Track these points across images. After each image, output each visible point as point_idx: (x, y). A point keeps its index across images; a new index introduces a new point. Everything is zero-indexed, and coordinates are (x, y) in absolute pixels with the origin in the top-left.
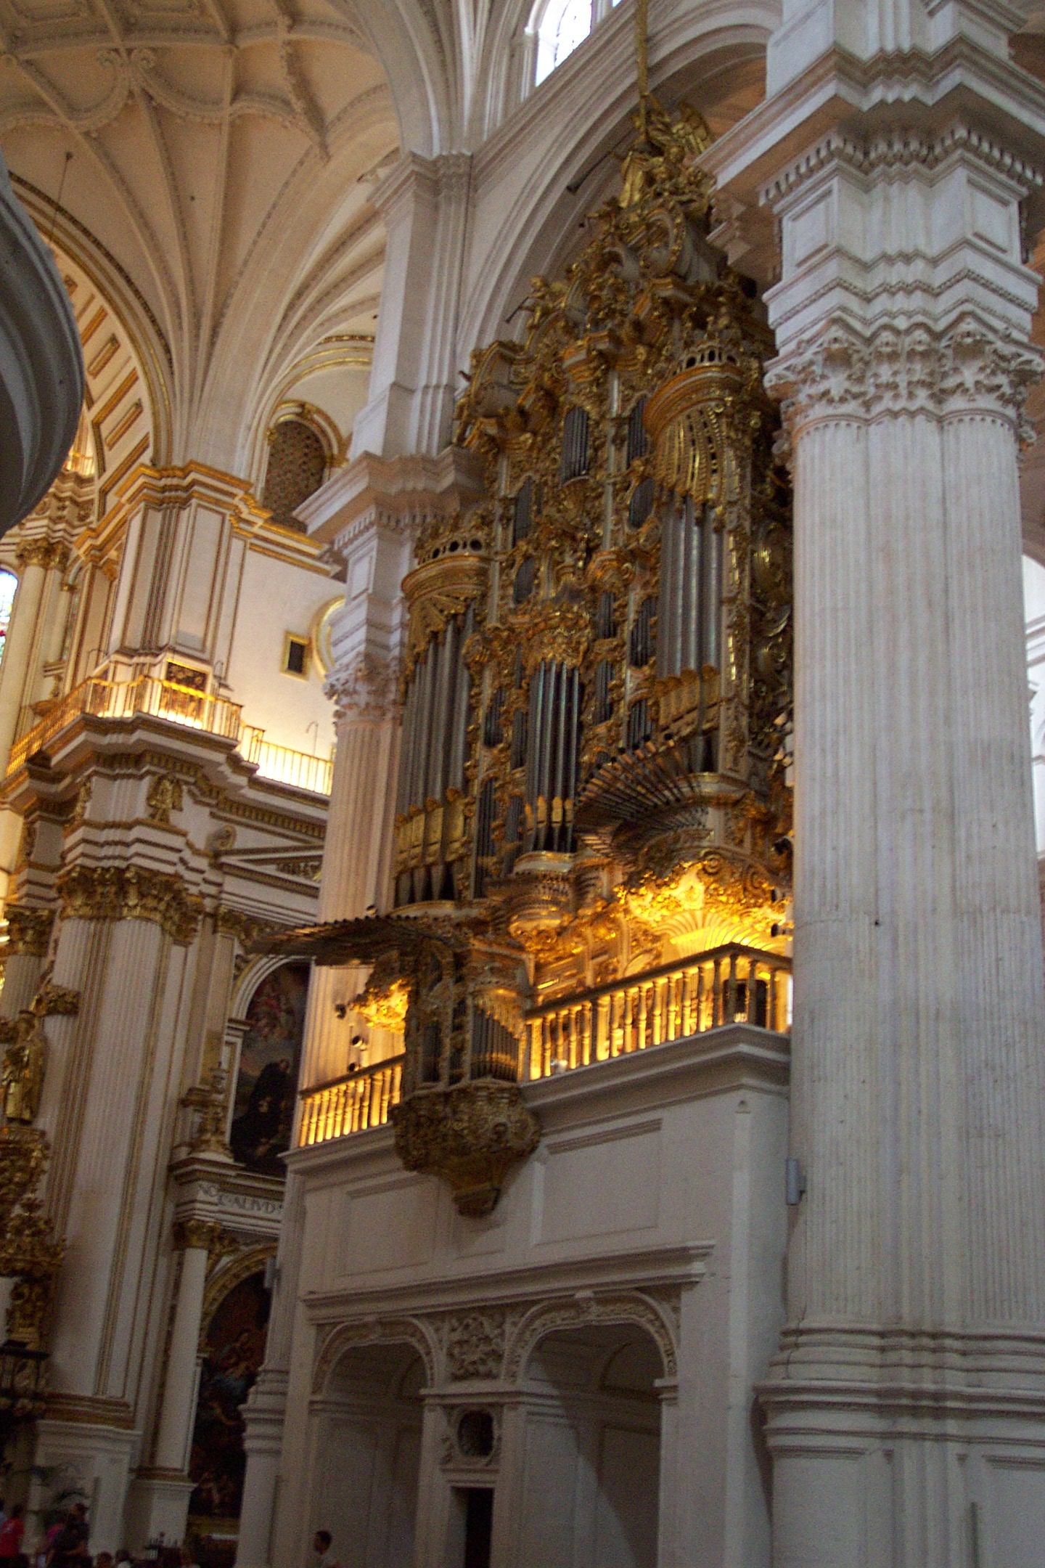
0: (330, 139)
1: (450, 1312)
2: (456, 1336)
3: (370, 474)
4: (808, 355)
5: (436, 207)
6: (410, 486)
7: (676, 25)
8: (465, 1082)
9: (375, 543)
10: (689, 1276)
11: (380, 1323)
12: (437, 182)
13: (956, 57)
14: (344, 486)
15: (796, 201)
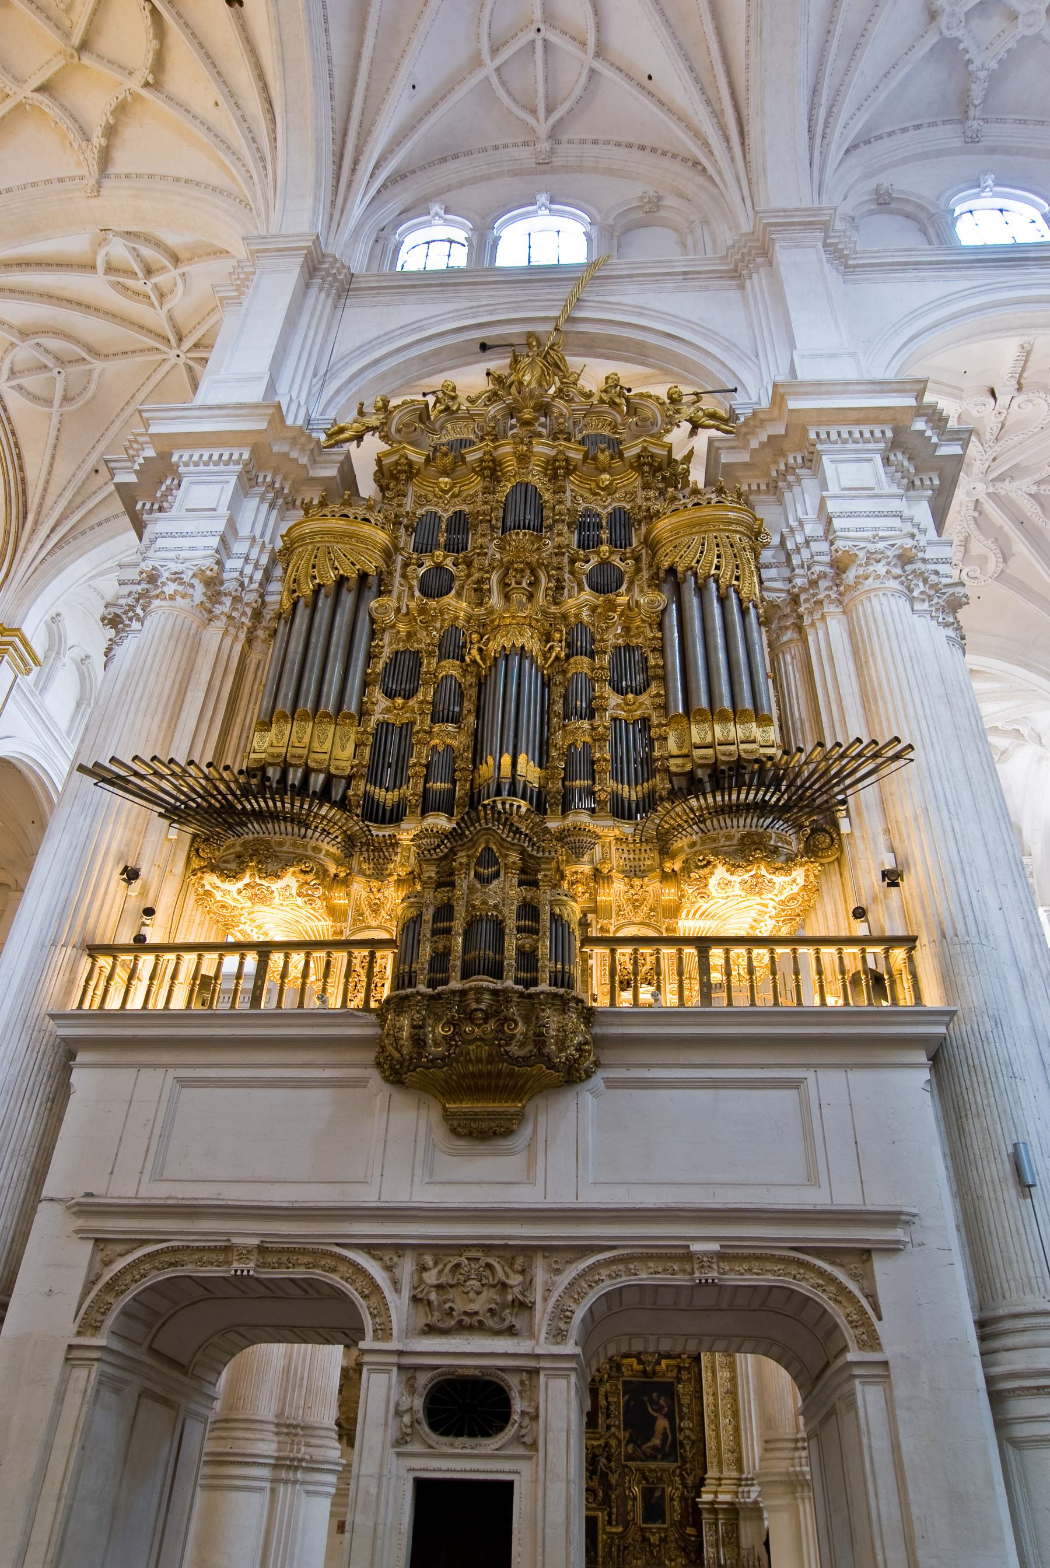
0: (107, 183)
1: (413, 1247)
2: (431, 1277)
3: (269, 422)
4: (881, 545)
5: (307, 286)
6: (294, 454)
7: (606, 306)
8: (544, 987)
9: (233, 480)
10: (898, 1242)
11: (262, 1249)
12: (315, 269)
13: (960, 439)
14: (228, 416)
15: (840, 452)
